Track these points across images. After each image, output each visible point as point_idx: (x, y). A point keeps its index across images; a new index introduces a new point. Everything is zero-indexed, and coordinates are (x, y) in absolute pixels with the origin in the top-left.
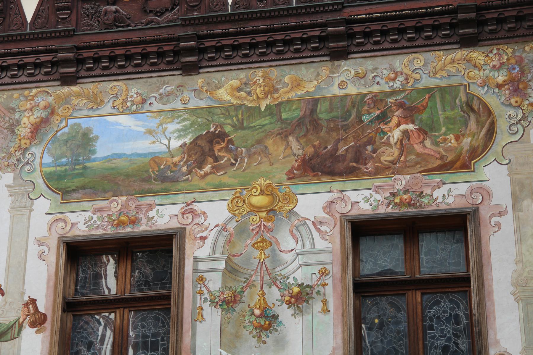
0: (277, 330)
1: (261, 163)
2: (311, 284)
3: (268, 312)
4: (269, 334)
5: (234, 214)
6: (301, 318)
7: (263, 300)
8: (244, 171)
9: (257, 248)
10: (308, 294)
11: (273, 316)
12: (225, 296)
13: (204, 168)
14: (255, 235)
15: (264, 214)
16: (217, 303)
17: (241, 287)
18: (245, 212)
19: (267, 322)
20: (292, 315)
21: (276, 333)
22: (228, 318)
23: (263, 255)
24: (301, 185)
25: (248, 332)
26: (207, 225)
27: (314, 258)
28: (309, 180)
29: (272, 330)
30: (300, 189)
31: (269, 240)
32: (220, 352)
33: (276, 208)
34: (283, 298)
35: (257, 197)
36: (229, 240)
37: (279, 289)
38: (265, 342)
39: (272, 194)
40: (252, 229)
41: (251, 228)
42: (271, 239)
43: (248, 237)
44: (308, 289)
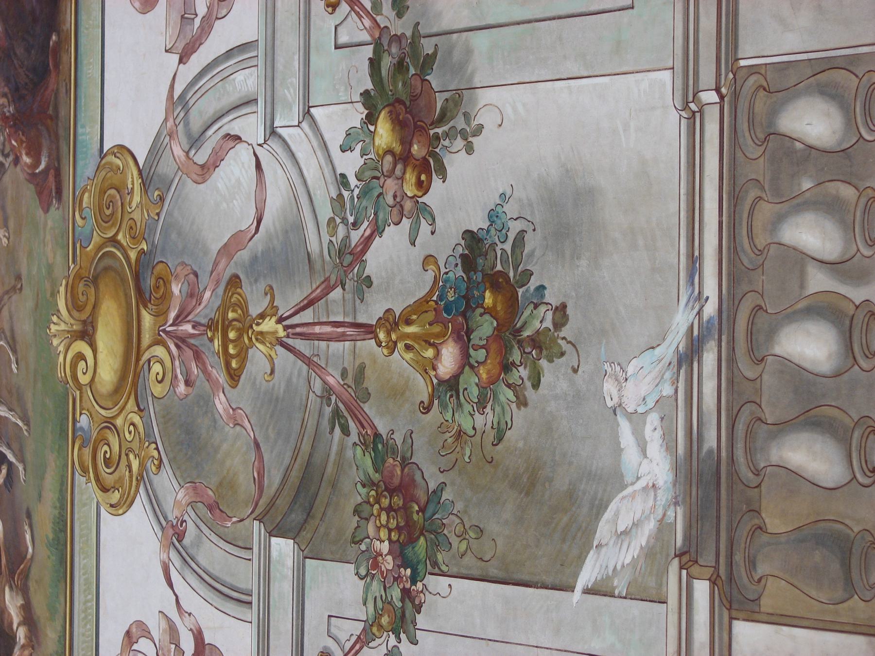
0: (520, 240)
1: (13, 337)
2: (368, 52)
3: (451, 296)
4: (533, 284)
5: (140, 478)
6: (485, 97)
7: (408, 323)
8: (27, 424)
9: (243, 356)
10: (400, 66)
11: (468, 262)
12: (385, 547)
13: (11, 623)
14: (205, 371)
15: (147, 319)
16: (406, 593)
17: (359, 450)
18: (137, 419)
20: (469, 149)
21: (532, 242)
22: (461, 536)
23: (269, 325)
24: (80, 130)
25: (520, 417)
26: (164, 624)
27: (289, 43)
28: (68, 91)
29: (516, 269)
30: (87, 133)
32: (587, 591)
33: (133, 255)
34: (408, 205)
35: (101, 356)
36: (210, 508)
37: (377, 230)
38: (561, 312)
39: (95, 281)
40: (187, 383)
41: (181, 388)
42: (218, 283)
43: (205, 403)
44: (387, 63)
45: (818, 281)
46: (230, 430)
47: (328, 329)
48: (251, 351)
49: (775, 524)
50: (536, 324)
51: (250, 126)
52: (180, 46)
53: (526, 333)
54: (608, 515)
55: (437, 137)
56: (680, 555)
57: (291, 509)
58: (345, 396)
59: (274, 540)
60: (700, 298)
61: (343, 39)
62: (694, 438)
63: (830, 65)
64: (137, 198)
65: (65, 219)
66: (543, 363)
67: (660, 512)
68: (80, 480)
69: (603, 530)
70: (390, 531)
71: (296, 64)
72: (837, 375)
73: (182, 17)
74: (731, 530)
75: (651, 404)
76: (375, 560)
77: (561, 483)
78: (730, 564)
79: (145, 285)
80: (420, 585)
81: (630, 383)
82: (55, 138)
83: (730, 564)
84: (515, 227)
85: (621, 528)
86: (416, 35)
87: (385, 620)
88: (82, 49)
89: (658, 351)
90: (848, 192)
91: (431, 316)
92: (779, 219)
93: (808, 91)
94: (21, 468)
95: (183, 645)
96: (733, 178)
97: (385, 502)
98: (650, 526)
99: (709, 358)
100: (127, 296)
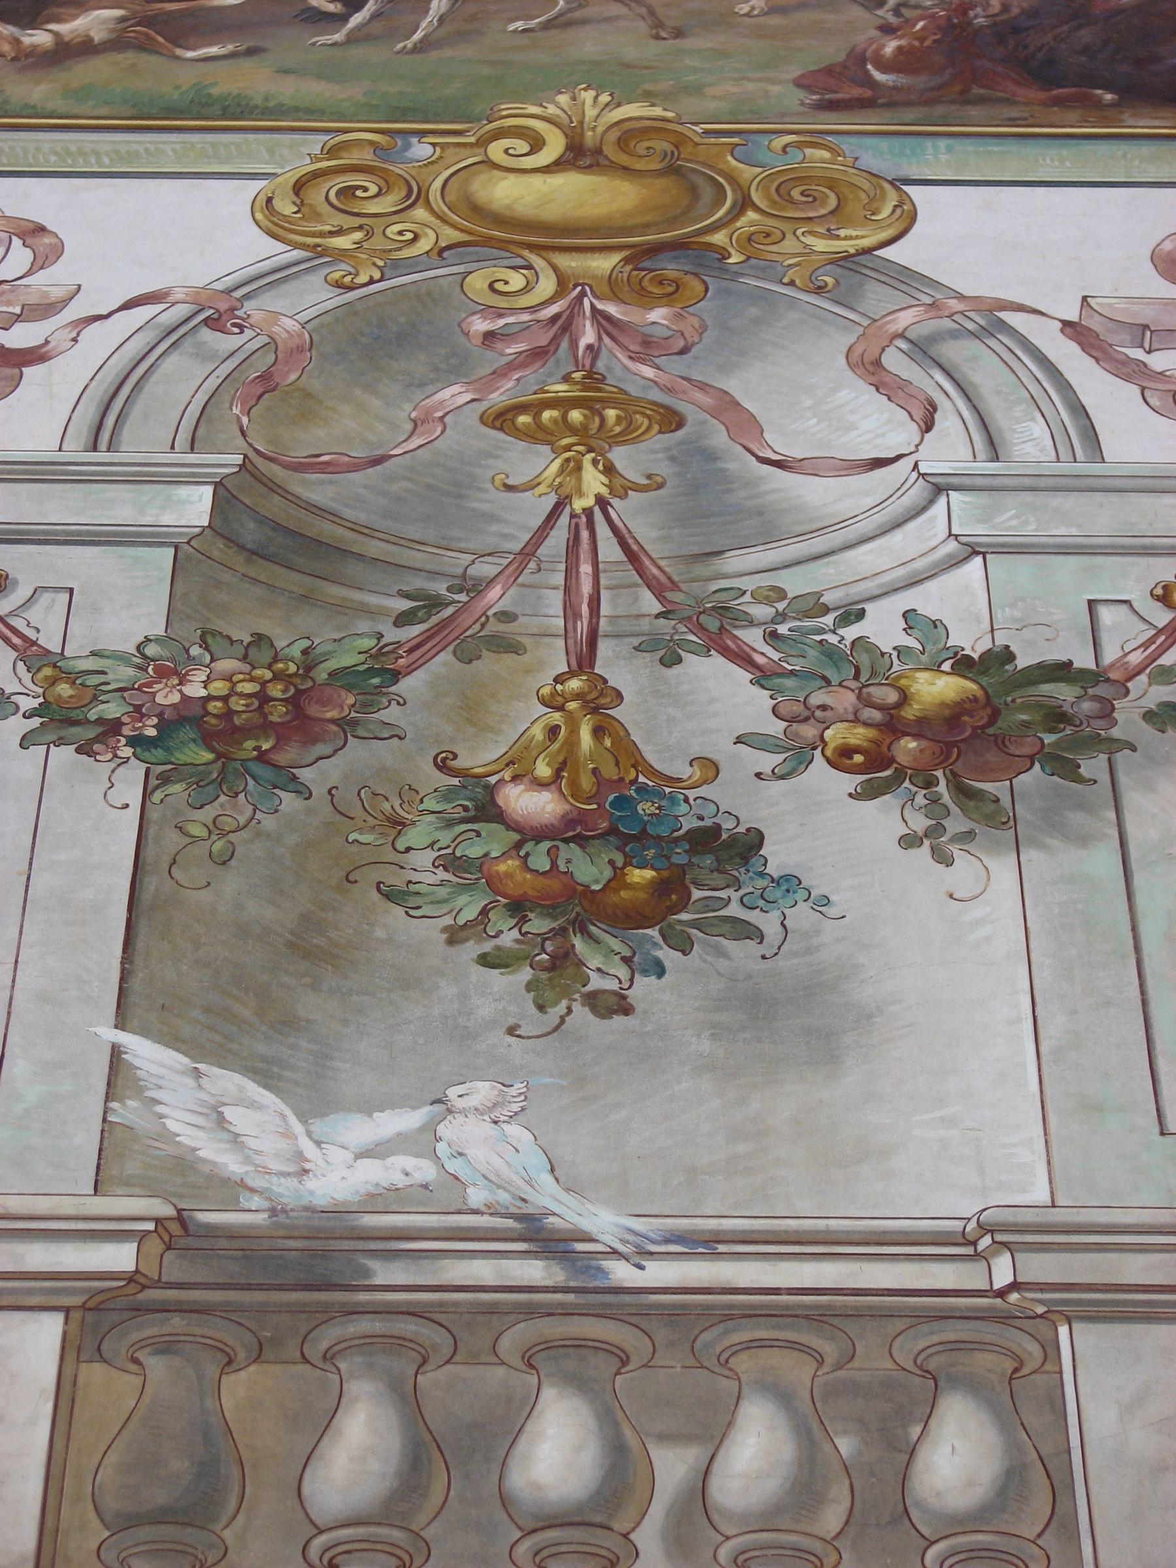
0: (747, 932)
1: (570, 24)
2: (1084, 660)
3: (645, 808)
4: (667, 955)
5: (319, 251)
6: (1003, 869)
7: (598, 732)
8: (417, 49)
9: (538, 435)
10: (1057, 717)
11: (706, 839)
12: (195, 690)
13: (59, 20)
14: (511, 367)
15: (604, 264)
16: (113, 727)
18: (424, 245)
19: (640, 876)
20: (909, 841)
21: (742, 952)
23: (593, 481)
24: (942, 143)
25: (428, 931)
26: (57, 293)
27: (1099, 517)
28: (1012, 122)
29: (695, 924)
30: (936, 157)
31: (656, 395)
32: (116, 1052)
33: (719, 238)
34: (809, 731)
35: (537, 181)
36: (265, 377)
37: (763, 676)
38: (616, 1005)
39: (673, 170)
40: (489, 336)
41: (480, 325)
42: (669, 390)
43: (454, 368)
44: (1063, 693)
45: (672, 1467)
46: (405, 412)
47: (586, 588)
48: (546, 449)
49: (237, 1389)
50: (594, 962)
51: (950, 448)
52: (1094, 323)
53: (578, 943)
54: (254, 1090)
55: (930, 783)
56: (181, 1218)
57: (263, 521)
58: (466, 619)
59: (208, 491)
60: (641, 1255)
61: (1106, 615)
62: (392, 1244)
63: (1060, 1488)
64: (820, 245)
65: (782, 116)
66: (526, 974)
67: (258, 1182)
68: (316, 143)
69: (226, 1081)
70: (225, 699)
71: (1061, 531)
72: (505, 1500)
73: (1146, 327)
74: (224, 1311)
75: (452, 1166)
76: (172, 672)
77: (310, 1006)
78: (165, 1309)
79: (665, 259)
80: (127, 752)
81: (488, 1129)
82: (928, 99)
83: (165, 1309)
84: (769, 923)
85: (229, 1113)
86: (1113, 746)
87: (64, 689)
88: (1087, 147)
89: (547, 1179)
90: (831, 1519)
91: (610, 771)
92: (784, 1397)
93: (1012, 1447)
94: (338, 37)
95: (19, 328)
96: (857, 1314)
97: (276, 691)
98: (233, 1165)
99: (534, 1271)
100: (645, 228)
